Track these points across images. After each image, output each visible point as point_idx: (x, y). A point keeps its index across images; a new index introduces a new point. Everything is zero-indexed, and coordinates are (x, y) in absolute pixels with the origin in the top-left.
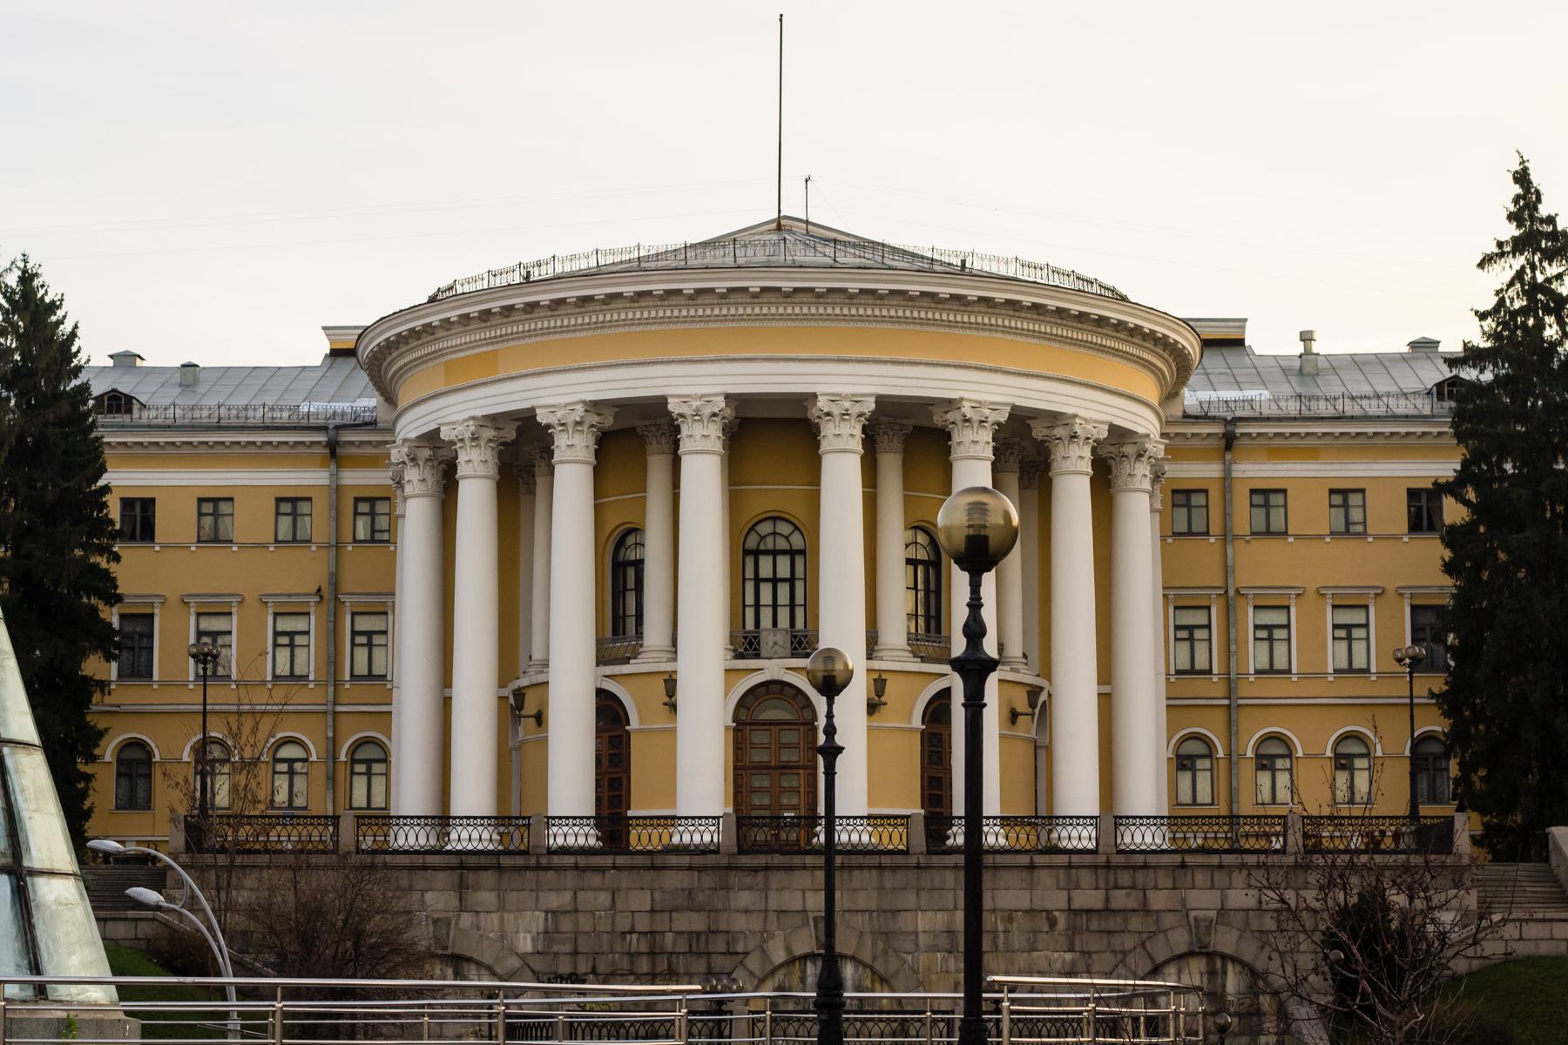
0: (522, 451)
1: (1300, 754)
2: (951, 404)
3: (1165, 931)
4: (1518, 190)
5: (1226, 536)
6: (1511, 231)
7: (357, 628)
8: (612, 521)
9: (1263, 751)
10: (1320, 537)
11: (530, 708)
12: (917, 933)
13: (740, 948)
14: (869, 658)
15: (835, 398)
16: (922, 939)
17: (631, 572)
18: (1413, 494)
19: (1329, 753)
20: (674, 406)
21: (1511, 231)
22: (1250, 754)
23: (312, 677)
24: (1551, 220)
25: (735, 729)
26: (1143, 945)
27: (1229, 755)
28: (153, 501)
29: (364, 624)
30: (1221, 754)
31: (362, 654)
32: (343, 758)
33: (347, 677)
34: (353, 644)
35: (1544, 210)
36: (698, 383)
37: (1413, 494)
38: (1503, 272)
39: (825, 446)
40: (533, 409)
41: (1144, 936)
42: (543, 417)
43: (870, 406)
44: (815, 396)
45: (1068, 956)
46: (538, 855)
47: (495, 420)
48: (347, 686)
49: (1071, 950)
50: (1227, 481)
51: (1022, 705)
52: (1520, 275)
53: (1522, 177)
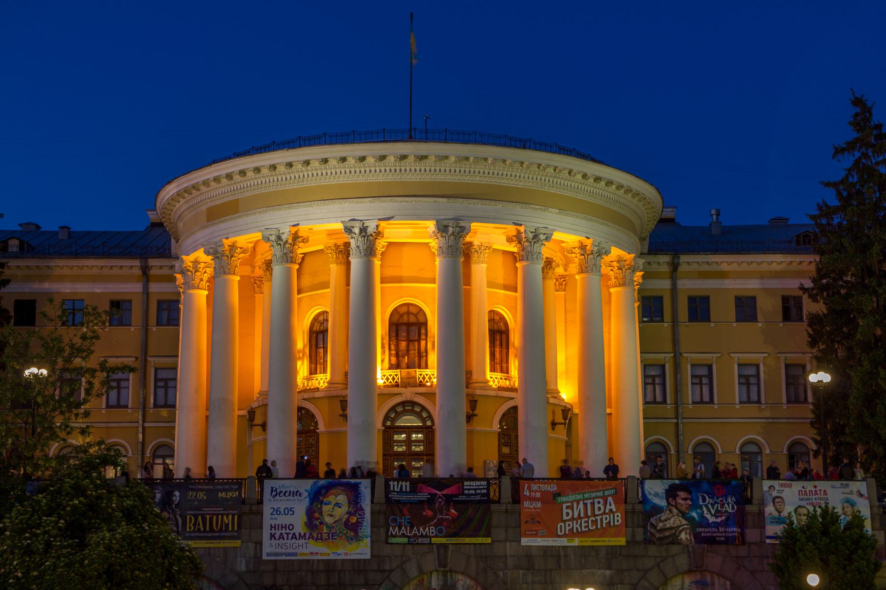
1: (720, 452)
3: (673, 556)
5: (675, 321)
6: (852, 134)
7: (159, 377)
9: (697, 450)
11: (258, 420)
12: (506, 557)
13: (387, 567)
14: (467, 387)
16: (510, 561)
19: (738, 452)
21: (852, 134)
22: (690, 452)
23: (130, 406)
25: (384, 432)
26: (658, 564)
27: (678, 452)
28: (35, 301)
29: (162, 375)
30: (673, 452)
31: (161, 392)
32: (148, 454)
33: (152, 406)
34: (156, 387)
37: (785, 299)
38: (848, 160)
41: (658, 560)
45: (608, 573)
46: (251, 505)
48: (152, 411)
49: (609, 568)
50: (674, 290)
51: (559, 419)
52: (857, 162)
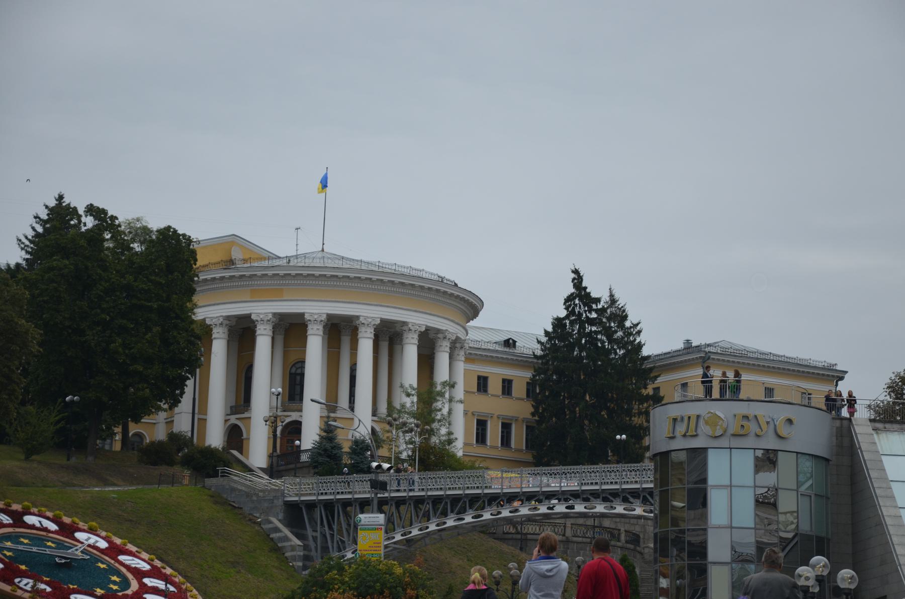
0: (291, 330)
2: (438, 331)
4: (573, 275)
8: (293, 358)
10: (474, 393)
15: (414, 324)
17: (298, 378)
18: (504, 381)
20: (361, 319)
24: (586, 288)
35: (584, 285)
36: (370, 313)
39: (405, 341)
40: (303, 315)
42: (307, 317)
43: (423, 329)
44: (404, 323)
47: (274, 314)
53: (576, 272)
